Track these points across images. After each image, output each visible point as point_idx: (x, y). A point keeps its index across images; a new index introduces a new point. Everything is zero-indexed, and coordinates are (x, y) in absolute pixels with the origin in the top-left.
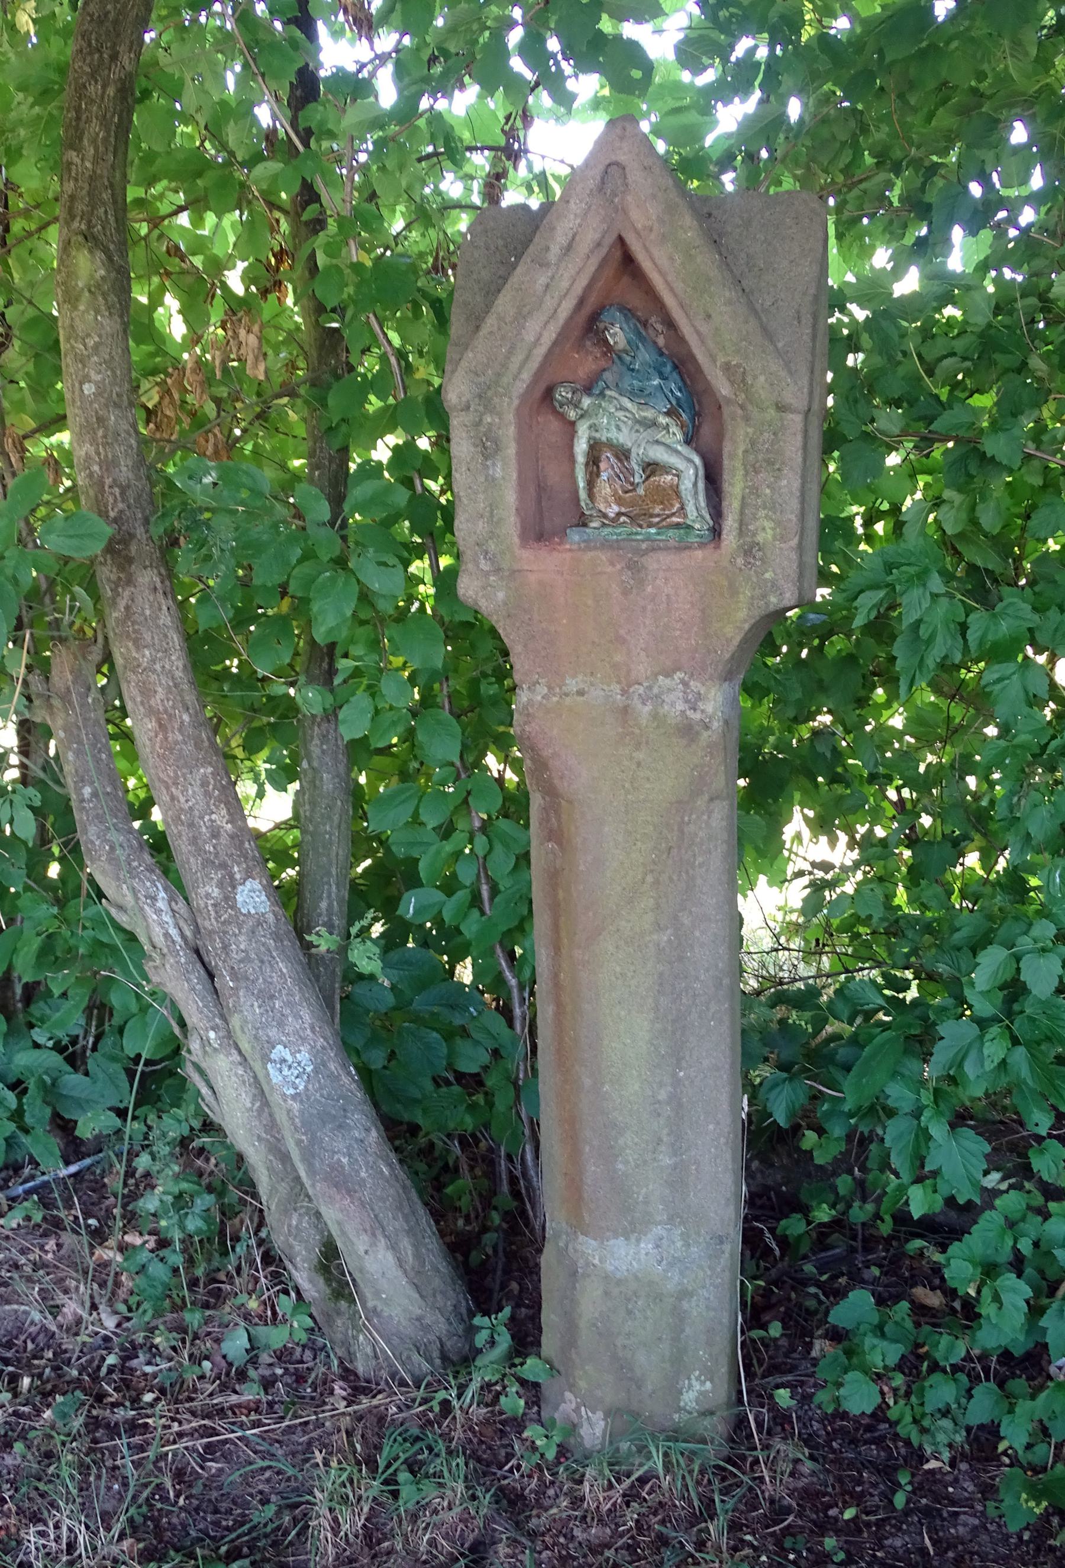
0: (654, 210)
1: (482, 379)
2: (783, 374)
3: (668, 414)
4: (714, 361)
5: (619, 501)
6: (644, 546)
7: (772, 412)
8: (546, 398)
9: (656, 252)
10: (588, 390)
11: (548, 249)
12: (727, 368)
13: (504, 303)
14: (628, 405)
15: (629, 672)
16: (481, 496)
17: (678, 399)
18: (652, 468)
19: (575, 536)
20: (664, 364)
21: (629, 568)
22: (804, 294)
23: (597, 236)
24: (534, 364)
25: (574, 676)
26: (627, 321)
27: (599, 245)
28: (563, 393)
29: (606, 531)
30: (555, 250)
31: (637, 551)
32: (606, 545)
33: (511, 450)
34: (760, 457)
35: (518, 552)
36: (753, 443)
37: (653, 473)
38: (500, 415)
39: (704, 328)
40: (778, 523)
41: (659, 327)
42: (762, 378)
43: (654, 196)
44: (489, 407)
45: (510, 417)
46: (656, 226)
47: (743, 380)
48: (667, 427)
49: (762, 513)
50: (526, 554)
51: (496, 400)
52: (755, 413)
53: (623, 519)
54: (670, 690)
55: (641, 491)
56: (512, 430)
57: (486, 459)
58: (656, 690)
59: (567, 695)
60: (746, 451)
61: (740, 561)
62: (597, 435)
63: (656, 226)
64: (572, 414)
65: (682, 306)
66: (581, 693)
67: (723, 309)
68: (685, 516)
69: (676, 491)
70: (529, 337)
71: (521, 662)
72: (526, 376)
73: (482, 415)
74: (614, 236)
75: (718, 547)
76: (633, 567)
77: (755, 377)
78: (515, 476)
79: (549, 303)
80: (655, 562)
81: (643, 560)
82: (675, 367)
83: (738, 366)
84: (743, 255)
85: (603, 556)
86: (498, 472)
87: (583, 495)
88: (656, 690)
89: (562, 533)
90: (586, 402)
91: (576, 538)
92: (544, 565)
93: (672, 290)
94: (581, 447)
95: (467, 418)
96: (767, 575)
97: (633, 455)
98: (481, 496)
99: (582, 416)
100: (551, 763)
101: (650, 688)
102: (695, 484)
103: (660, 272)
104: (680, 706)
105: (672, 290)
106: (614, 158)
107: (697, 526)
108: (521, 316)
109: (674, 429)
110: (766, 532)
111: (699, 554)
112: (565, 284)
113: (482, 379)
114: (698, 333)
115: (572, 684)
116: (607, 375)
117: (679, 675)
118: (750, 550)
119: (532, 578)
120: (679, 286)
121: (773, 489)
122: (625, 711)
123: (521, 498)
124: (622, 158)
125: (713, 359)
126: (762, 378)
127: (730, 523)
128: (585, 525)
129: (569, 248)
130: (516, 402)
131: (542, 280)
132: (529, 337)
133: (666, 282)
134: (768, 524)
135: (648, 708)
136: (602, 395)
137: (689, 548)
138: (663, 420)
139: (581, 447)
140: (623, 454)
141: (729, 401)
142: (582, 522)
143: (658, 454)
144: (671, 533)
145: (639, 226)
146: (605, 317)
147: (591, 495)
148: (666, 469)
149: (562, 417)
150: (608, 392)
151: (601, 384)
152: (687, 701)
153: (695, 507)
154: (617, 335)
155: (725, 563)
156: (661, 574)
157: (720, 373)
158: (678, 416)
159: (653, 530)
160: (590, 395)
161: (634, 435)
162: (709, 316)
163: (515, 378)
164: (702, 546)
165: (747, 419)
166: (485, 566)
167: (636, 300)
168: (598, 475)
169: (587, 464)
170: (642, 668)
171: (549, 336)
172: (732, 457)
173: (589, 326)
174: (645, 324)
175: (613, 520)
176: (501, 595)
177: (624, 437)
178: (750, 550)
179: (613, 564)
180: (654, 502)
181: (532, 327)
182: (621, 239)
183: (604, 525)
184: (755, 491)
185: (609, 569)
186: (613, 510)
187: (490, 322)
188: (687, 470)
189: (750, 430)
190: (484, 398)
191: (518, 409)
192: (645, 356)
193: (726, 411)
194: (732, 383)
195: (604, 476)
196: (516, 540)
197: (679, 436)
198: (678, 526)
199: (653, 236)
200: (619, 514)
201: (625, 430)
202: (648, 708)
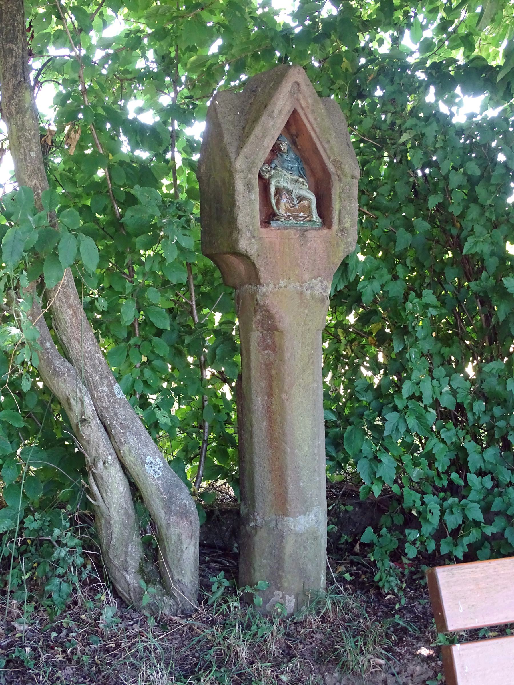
0: (310, 101)
1: (249, 160)
9: (310, 117)
11: (273, 112)
12: (334, 162)
15: (302, 278)
16: (248, 207)
18: (301, 198)
25: (282, 280)
30: (276, 112)
34: (346, 195)
35: (261, 229)
39: (326, 146)
40: (352, 220)
46: (310, 107)
48: (303, 183)
49: (347, 216)
52: (344, 179)
54: (316, 285)
55: (297, 207)
58: (311, 285)
59: (281, 287)
60: (340, 193)
61: (339, 234)
63: (310, 107)
65: (318, 137)
66: (286, 287)
71: (263, 275)
81: (305, 233)
86: (253, 197)
88: (311, 285)
91: (275, 225)
94: (273, 190)
95: (242, 175)
98: (248, 207)
100: (275, 316)
101: (309, 284)
104: (320, 291)
108: (264, 136)
109: (306, 184)
113: (249, 160)
115: (282, 283)
117: (320, 278)
118: (342, 230)
119: (267, 240)
120: (318, 130)
122: (301, 293)
124: (298, 80)
125: (329, 158)
129: (280, 112)
134: (349, 220)
135: (309, 292)
138: (301, 180)
140: (289, 192)
141: (334, 174)
144: (308, 223)
148: (307, 199)
152: (322, 289)
161: (293, 185)
165: (340, 180)
166: (249, 235)
170: (306, 277)
176: (256, 247)
177: (290, 186)
178: (342, 230)
179: (295, 235)
184: (344, 207)
185: (294, 237)
187: (252, 138)
202: (309, 292)
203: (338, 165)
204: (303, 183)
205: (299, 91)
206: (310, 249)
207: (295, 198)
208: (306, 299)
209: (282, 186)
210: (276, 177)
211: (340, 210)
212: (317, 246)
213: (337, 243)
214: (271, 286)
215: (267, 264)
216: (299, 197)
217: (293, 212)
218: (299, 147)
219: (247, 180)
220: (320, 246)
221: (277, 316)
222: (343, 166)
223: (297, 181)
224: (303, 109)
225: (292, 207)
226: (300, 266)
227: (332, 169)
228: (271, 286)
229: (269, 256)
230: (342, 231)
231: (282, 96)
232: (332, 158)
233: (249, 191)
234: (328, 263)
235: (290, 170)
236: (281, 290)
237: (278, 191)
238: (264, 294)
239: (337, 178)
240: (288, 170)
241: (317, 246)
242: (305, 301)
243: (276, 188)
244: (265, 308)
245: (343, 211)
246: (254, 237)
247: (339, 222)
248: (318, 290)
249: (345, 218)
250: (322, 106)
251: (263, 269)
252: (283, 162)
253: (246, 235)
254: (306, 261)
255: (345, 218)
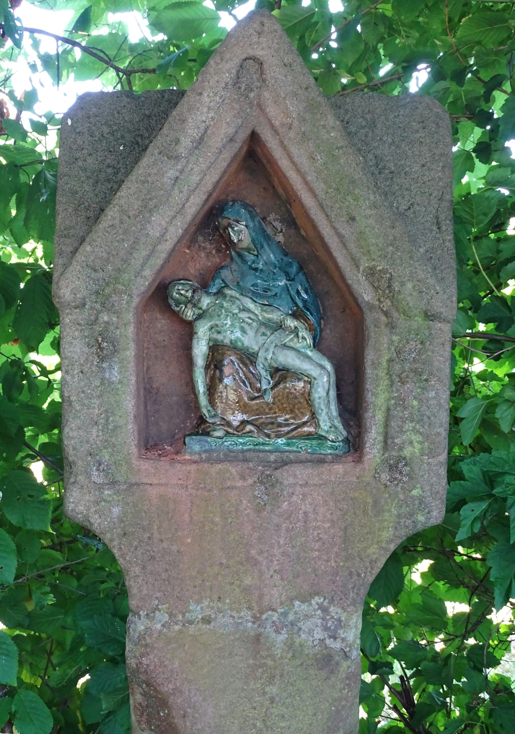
0: (294, 107)
1: (100, 275)
2: (431, 281)
3: (295, 315)
4: (358, 267)
5: (244, 408)
6: (272, 457)
7: (420, 319)
8: (160, 295)
9: (294, 150)
10: (204, 286)
11: (177, 141)
13: (128, 195)
14: (251, 305)
15: (261, 597)
17: (304, 301)
18: (281, 374)
19: (195, 444)
20: (290, 265)
21: (262, 483)
22: (441, 199)
23: (231, 131)
24: (158, 261)
25: (199, 602)
26: (252, 218)
27: (232, 140)
28: (180, 291)
29: (228, 442)
30: (186, 143)
31: (267, 464)
32: (231, 457)
33: (130, 353)
34: (407, 366)
35: (135, 462)
36: (398, 352)
37: (283, 379)
38: (118, 313)
39: (345, 230)
40: (427, 437)
41: (278, 225)
42: (409, 285)
43: (295, 94)
44: (106, 305)
45: (130, 317)
46: (296, 123)
47: (389, 287)
48: (295, 331)
49: (409, 426)
50: (145, 466)
51: (115, 298)
52: (401, 321)
53: (249, 428)
54: (307, 617)
55: (269, 398)
56: (131, 330)
57: (102, 360)
58: (291, 617)
59: (191, 622)
60: (390, 361)
61: (385, 477)
62: (220, 337)
63: (296, 123)
64: (189, 314)
66: (207, 620)
67: (369, 212)
68: (317, 426)
69: (307, 397)
70: (154, 232)
71: (137, 587)
72: (148, 273)
73: (99, 312)
74: (248, 132)
75: (359, 460)
76: (267, 481)
77: (403, 284)
78: (133, 379)
79: (177, 197)
80: (293, 477)
81: (278, 473)
82: (301, 268)
83: (384, 271)
84: (370, 156)
85: (233, 470)
86: (115, 374)
87: (203, 400)
88: (291, 617)
89: (178, 444)
90: (206, 301)
91: (197, 448)
92: (166, 479)
93: (311, 190)
94: (200, 349)
95: (81, 316)
96: (415, 492)
97: (260, 360)
98: (96, 402)
99: (200, 317)
100: (171, 700)
101: (285, 614)
102: (328, 393)
103: (298, 171)
104: (319, 634)
105: (311, 190)
106: (251, 52)
107: (331, 437)
108: (147, 209)
109: (303, 333)
110: (413, 445)
111: (339, 468)
112: (195, 178)
113: (100, 275)
114: (340, 236)
115: (196, 611)
116: (225, 273)
117: (318, 600)
118: (395, 466)
119: (153, 492)
120: (319, 187)
121: (420, 401)
122: (257, 638)
123: (137, 406)
124: (259, 53)
126: (409, 285)
127: (373, 436)
128: (208, 434)
129: (200, 142)
130: (136, 301)
131: (172, 173)
132: (154, 232)
133: (306, 183)
135: (283, 637)
136: (220, 293)
137: (322, 461)
138: (291, 323)
139: (200, 349)
140: (248, 358)
141: (372, 308)
142: (201, 427)
143: (290, 359)
144: (302, 444)
145: (277, 123)
146: (230, 213)
147: (212, 402)
148: (297, 375)
149: (176, 316)
150: (228, 292)
151: (218, 282)
152: (326, 629)
153: (328, 418)
154: (241, 233)
155: (368, 478)
156: (298, 488)
157: (362, 279)
158: (306, 320)
159: (281, 441)
160: (208, 294)
161: (261, 339)
162: (353, 219)
163: (138, 274)
164: (337, 459)
165: (392, 326)
166: (97, 478)
167: (254, 195)
168: (221, 380)
169: (207, 367)
170: (275, 594)
171: (177, 231)
172: (376, 365)
173: (211, 223)
174: (264, 219)
175: (237, 429)
176: (116, 511)
177: (250, 341)
178: (395, 466)
179: (243, 478)
180: (283, 410)
181: (158, 221)
182: (254, 138)
183: (228, 433)
185: (240, 484)
186: (237, 418)
187: (112, 214)
188: (320, 377)
189: (395, 338)
190: (103, 295)
191: (137, 308)
192: (270, 255)
193: (370, 318)
194: (376, 289)
195: (227, 381)
196: (134, 450)
197: (309, 341)
198: (309, 436)
199: (292, 134)
200: (243, 423)
201: (251, 333)
202: (283, 637)
203: (384, 284)
204: (295, 331)
205: (264, 81)
206: (288, 516)
207: (263, 373)
208: (272, 657)
209: (227, 341)
210: (211, 317)
211: (388, 410)
212: (309, 508)
213: (376, 503)
214: (163, 617)
215: (153, 558)
216: (277, 370)
217: (259, 412)
218: (303, 233)
219: (97, 328)
220: (322, 510)
221: (175, 701)
222: (396, 286)
223: (280, 327)
224: (276, 132)
225: (253, 399)
226: (256, 563)
227: (366, 294)
228: (163, 617)
229: (156, 535)
230: (392, 468)
231: (205, 99)
232: (365, 264)
233: (102, 360)
234: (348, 558)
235: (262, 297)
236: (192, 629)
237: (217, 353)
238: (142, 637)
239: (383, 318)
240: (255, 296)
241: (309, 508)
242: (270, 662)
243: (210, 348)
244: (143, 677)
245: (397, 412)
246: (113, 483)
247: (385, 442)
248: (310, 632)
249: (402, 431)
250: (331, 120)
251: (136, 570)
252: (243, 275)
253: (89, 476)
254: (276, 551)
255: (402, 431)
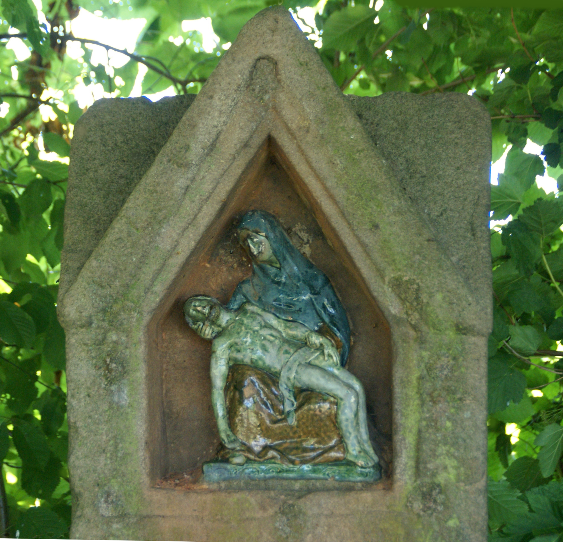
0: (311, 110)
1: (108, 291)
2: (463, 292)
3: (321, 332)
4: (383, 277)
5: (266, 432)
6: (297, 485)
7: (451, 334)
8: (176, 312)
9: (313, 155)
10: (225, 303)
11: (187, 148)
12: (398, 285)
13: (136, 205)
14: (274, 322)
16: (104, 428)
17: (331, 316)
18: (305, 394)
19: (213, 473)
20: (315, 278)
21: (283, 513)
22: (476, 204)
23: (245, 135)
24: (169, 275)
26: (273, 228)
27: (246, 145)
28: (197, 308)
29: (250, 469)
31: (290, 492)
32: (252, 485)
33: (140, 373)
34: (439, 384)
36: (429, 369)
37: (307, 400)
38: (128, 333)
39: (369, 239)
40: (462, 461)
41: (304, 236)
42: (439, 297)
43: (311, 95)
44: (114, 323)
45: (139, 335)
46: (313, 127)
47: (417, 298)
48: (321, 348)
49: (442, 449)
50: (158, 496)
51: (123, 315)
52: (431, 334)
53: (271, 453)
55: (292, 421)
56: (141, 351)
57: (111, 383)
60: (421, 378)
61: (418, 506)
62: (239, 356)
63: (313, 127)
64: (208, 332)
65: (343, 214)
67: (393, 219)
68: (346, 450)
69: (334, 420)
70: (165, 244)
72: (160, 289)
73: (106, 332)
74: (264, 136)
75: (389, 488)
76: (289, 512)
77: (431, 295)
78: (144, 403)
79: (188, 208)
81: (301, 503)
82: (327, 281)
83: (411, 282)
84: (401, 160)
85: (252, 499)
86: (125, 398)
87: (222, 424)
89: (196, 471)
90: (225, 318)
91: (215, 476)
93: (331, 197)
94: (219, 370)
95: (89, 335)
96: (452, 523)
97: (283, 380)
98: (104, 428)
99: (219, 335)
102: (356, 415)
103: (317, 176)
105: (331, 197)
106: (265, 52)
107: (361, 462)
108: (156, 221)
109: (329, 350)
110: (448, 472)
111: (367, 496)
112: (207, 187)
113: (108, 291)
114: (363, 245)
116: (247, 288)
118: (429, 493)
120: (340, 193)
121: (454, 422)
123: (150, 430)
124: (273, 52)
125: (381, 273)
126: (439, 297)
127: (404, 461)
128: (226, 461)
129: (212, 147)
130: (147, 318)
131: (182, 182)
132: (165, 244)
133: (326, 189)
134: (451, 463)
136: (241, 310)
137: (350, 489)
138: (316, 340)
139: (219, 370)
140: (270, 378)
141: (399, 321)
142: (221, 455)
143: (314, 379)
144: (329, 471)
145: (294, 126)
146: (248, 224)
147: (232, 425)
149: (195, 334)
150: (249, 308)
151: (240, 298)
153: (357, 442)
154: (261, 245)
155: (399, 508)
156: (323, 520)
157: (388, 290)
158: (333, 336)
159: (306, 467)
160: (228, 310)
162: (376, 227)
163: (147, 290)
164: (367, 486)
165: (421, 341)
166: (106, 510)
167: (277, 204)
168: (241, 402)
169: (226, 389)
171: (188, 243)
172: (405, 383)
173: (229, 233)
174: (289, 230)
175: (259, 455)
177: (271, 359)
178: (429, 493)
179: (263, 508)
180: (308, 434)
181: (168, 234)
182: (270, 142)
183: (248, 460)
184: (433, 423)
185: (259, 514)
186: (258, 443)
187: (119, 226)
188: (348, 398)
189: (425, 354)
190: (110, 313)
191: (148, 326)
192: (293, 268)
193: (397, 332)
194: (403, 301)
195: (249, 403)
196: (145, 479)
197: (336, 359)
198: (336, 462)
199: (309, 138)
200: (266, 448)
201: (273, 351)
203: (411, 295)
205: (279, 81)
207: (286, 394)
209: (247, 360)
210: (231, 335)
211: (420, 431)
217: (282, 436)
218: (331, 244)
219: (106, 348)
222: (424, 298)
223: (304, 344)
225: (275, 422)
227: (393, 307)
231: (216, 101)
235: (285, 312)
237: (237, 372)
239: (412, 333)
240: (278, 311)
247: (417, 468)
252: (265, 290)
253: (96, 508)
255: (434, 455)
